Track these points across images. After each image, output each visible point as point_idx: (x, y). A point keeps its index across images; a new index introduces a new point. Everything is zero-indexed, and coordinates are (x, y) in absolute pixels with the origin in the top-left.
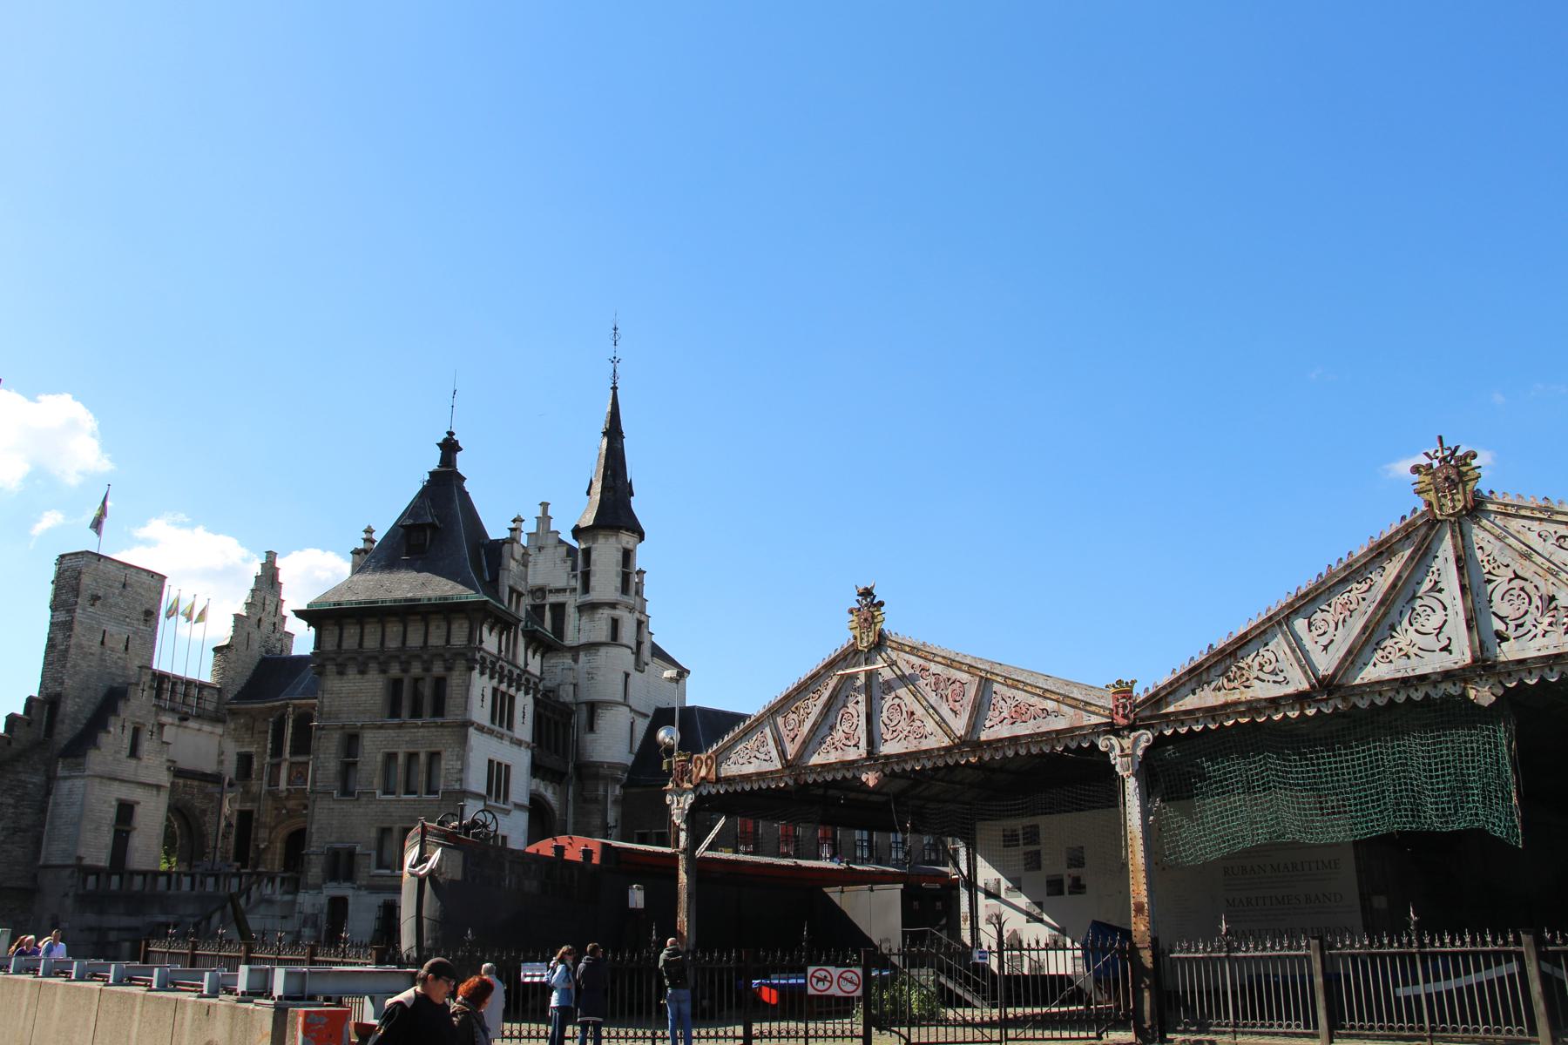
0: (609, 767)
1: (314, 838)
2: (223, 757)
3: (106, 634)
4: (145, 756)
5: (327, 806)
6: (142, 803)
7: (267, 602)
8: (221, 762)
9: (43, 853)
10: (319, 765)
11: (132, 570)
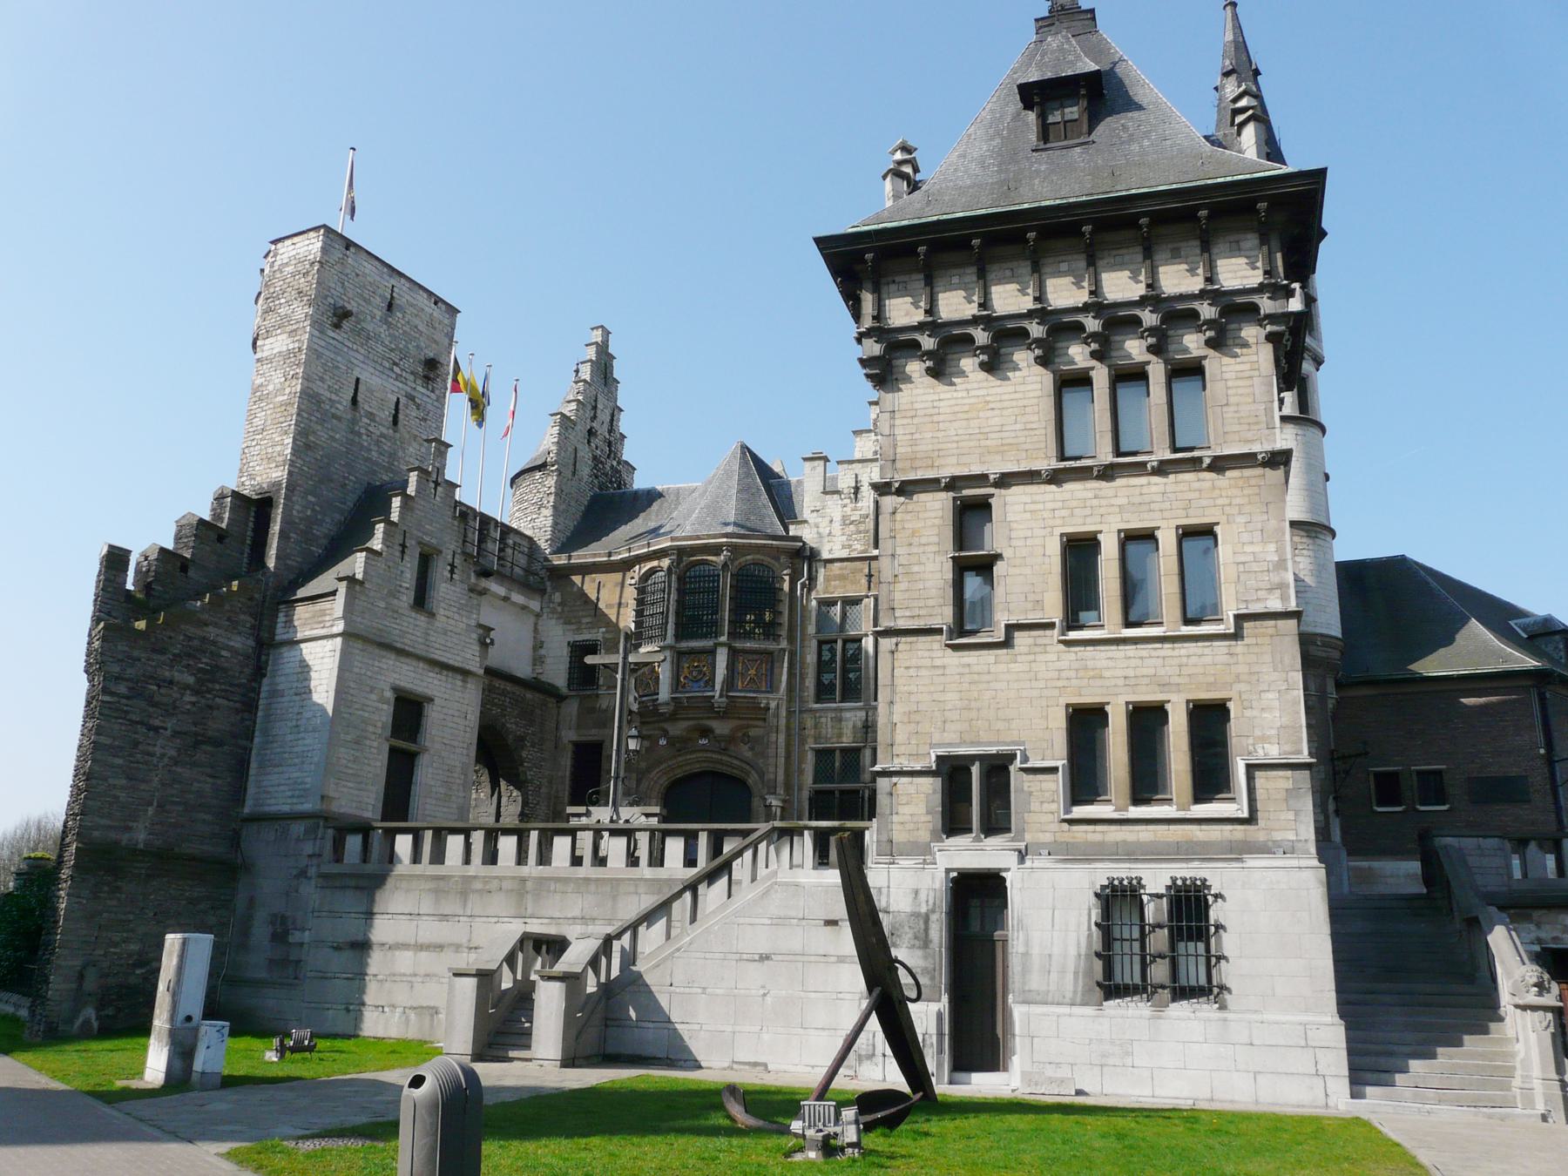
0: (1324, 645)
1: (900, 737)
2: (543, 652)
3: (362, 388)
4: (442, 612)
5: (927, 662)
6: (437, 701)
7: (600, 406)
8: (538, 660)
9: (251, 790)
10: (901, 570)
11: (403, 280)
